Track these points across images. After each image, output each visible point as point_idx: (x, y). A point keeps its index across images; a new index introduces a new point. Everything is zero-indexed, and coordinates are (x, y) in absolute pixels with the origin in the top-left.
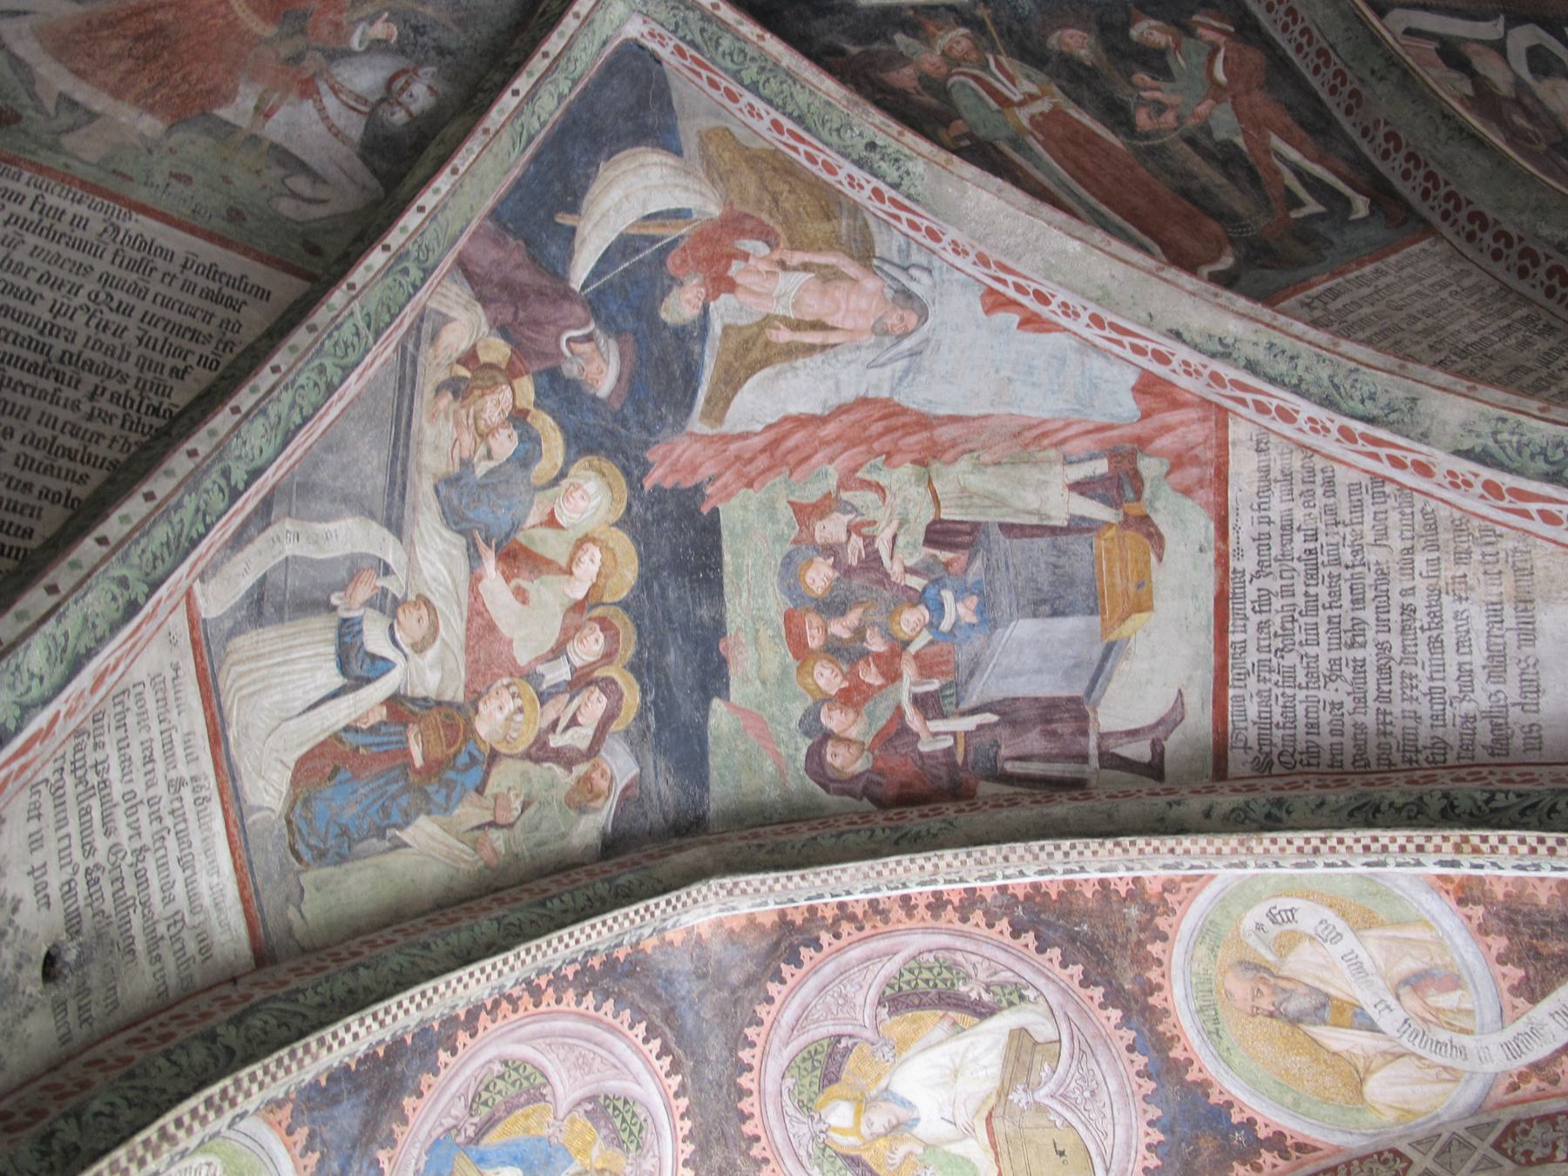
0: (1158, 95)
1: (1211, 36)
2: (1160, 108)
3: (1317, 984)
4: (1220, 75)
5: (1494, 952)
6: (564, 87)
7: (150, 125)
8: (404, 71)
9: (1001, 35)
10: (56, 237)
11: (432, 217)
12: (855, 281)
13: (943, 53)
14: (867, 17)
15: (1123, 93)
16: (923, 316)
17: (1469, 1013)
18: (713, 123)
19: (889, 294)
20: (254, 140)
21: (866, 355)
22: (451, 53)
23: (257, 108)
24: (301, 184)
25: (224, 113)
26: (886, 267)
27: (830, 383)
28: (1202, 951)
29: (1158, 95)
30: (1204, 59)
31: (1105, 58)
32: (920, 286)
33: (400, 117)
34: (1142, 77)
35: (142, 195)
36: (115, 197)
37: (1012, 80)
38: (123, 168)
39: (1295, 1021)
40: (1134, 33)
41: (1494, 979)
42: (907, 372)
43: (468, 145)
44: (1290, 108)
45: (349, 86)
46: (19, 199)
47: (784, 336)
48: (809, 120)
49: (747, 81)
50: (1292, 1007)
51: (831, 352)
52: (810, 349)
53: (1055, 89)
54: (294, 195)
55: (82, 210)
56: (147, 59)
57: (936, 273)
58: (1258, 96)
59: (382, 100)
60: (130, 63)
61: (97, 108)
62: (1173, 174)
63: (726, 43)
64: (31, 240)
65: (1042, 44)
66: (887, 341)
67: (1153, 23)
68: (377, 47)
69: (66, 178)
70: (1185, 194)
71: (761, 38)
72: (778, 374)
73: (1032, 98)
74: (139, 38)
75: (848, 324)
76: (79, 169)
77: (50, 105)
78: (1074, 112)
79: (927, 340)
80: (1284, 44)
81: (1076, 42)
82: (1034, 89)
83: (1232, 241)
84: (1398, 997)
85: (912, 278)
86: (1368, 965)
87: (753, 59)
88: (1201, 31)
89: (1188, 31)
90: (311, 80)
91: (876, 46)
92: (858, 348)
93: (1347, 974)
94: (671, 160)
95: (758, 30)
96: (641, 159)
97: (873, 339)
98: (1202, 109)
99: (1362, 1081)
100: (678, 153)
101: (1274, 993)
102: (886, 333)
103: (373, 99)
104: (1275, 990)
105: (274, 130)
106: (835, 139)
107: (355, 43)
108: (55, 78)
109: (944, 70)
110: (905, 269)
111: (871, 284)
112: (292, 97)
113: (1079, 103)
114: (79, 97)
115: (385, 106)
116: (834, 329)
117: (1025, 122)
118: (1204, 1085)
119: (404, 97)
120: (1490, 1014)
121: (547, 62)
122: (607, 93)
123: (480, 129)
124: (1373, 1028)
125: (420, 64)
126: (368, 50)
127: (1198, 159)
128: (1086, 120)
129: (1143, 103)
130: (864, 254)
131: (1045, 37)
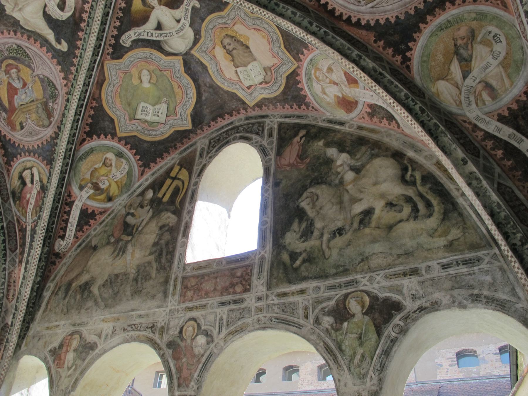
3: (474, 57)
5: (511, 106)
17: (485, 104)
28: (473, 15)
39: (457, 53)
41: (501, 108)
50: (462, 51)
84: (480, 82)
86: (488, 71)
93: (482, 65)
99: (443, 79)
101: (465, 44)
104: (466, 45)
118: (420, 31)
120: (486, 110)
124: (465, 77)
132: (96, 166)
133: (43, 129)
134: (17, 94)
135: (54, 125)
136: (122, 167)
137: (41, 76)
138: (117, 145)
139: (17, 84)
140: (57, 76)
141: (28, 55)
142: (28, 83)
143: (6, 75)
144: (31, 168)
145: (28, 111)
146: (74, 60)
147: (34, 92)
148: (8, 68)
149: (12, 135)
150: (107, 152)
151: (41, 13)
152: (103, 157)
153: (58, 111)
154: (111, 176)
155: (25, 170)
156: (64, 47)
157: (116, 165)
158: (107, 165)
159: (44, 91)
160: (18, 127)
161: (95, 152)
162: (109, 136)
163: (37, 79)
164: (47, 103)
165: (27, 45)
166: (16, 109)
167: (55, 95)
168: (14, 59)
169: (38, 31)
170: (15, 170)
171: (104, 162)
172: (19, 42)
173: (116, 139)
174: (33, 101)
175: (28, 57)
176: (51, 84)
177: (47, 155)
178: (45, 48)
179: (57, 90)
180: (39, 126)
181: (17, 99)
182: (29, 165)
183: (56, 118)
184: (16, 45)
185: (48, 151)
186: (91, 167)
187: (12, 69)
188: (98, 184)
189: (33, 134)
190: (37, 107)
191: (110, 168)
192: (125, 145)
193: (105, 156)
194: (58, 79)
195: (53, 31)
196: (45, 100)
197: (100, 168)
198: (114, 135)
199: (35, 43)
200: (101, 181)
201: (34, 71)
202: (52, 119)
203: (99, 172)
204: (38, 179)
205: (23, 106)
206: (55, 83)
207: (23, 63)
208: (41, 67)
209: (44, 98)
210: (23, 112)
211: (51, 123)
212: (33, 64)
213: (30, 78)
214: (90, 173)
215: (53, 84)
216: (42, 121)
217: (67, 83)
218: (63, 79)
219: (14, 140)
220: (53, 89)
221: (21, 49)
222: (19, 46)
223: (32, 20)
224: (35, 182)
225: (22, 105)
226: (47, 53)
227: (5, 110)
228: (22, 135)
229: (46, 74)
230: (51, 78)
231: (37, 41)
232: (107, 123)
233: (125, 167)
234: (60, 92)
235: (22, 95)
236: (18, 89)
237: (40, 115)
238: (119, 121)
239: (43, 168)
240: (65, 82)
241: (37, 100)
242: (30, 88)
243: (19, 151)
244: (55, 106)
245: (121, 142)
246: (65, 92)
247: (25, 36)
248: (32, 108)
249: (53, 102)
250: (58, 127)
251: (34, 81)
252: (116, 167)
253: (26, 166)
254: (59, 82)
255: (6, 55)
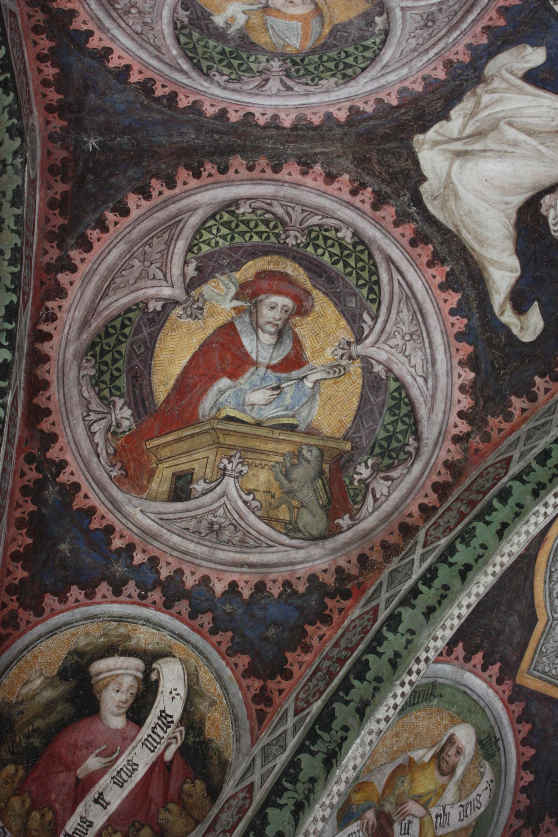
132: (416, 755)
133: (287, 540)
134: (234, 375)
135: (347, 544)
136: (474, 795)
137: (378, 368)
138: (499, 706)
139: (259, 346)
140: (440, 396)
141: (377, 282)
142: (312, 363)
143: (236, 297)
144: (150, 658)
145: (247, 450)
146: (537, 379)
147: (318, 402)
148: (264, 284)
149: (113, 501)
150: (464, 721)
151: (519, 200)
152: (446, 728)
153: (387, 507)
154: (434, 811)
155: (110, 650)
156: (529, 326)
157: (464, 776)
158: (444, 766)
159: (359, 415)
160: (161, 482)
161: (435, 702)
162: (494, 670)
163: (356, 368)
164: (349, 460)
165: (396, 254)
166: (192, 419)
167: (399, 450)
168: (314, 269)
169: (467, 237)
170: (52, 632)
171: (442, 750)
172: (370, 231)
173: (507, 686)
174: (292, 428)
175: (371, 291)
176: (404, 410)
177: (266, 639)
178: (457, 297)
179: (418, 439)
180: (268, 520)
181: (221, 392)
182: (144, 637)
183: (365, 525)
184: (355, 234)
185: (275, 624)
186: (403, 750)
187: (279, 293)
188: (391, 823)
189: (226, 535)
190: (298, 455)
191: (445, 779)
192: (519, 720)
193: (451, 731)
194: (440, 406)
195: (523, 266)
196: (348, 446)
197: (424, 766)
198: (509, 671)
199: (430, 264)
200: (404, 815)
201: (359, 340)
202: (345, 521)
203: (412, 780)
204: (175, 709)
205: (232, 426)
206: (423, 412)
207: (338, 299)
208: (398, 341)
209: (345, 438)
210: (220, 445)
211: (332, 531)
212: (375, 318)
213: (329, 354)
214: (389, 769)
215: (413, 412)
216: (291, 509)
217: (468, 435)
218: (461, 414)
219: (111, 519)
220: (401, 427)
221: (365, 257)
222: (362, 243)
223: (469, 199)
224: (152, 719)
225: (229, 419)
226: (452, 312)
227: (141, 401)
228: (164, 521)
229: (401, 369)
230: (415, 392)
231: (443, 262)
232: (514, 620)
233: (482, 793)
234: (426, 452)
235: (255, 388)
236: (255, 364)
237: (295, 486)
238: (547, 634)
239: (219, 678)
240: (464, 427)
241: (311, 432)
242: (308, 384)
243: (119, 569)
244: (381, 487)
245: (513, 707)
246: (444, 456)
247: (408, 229)
248: (270, 446)
249: (376, 469)
250: (363, 559)
251: (337, 370)
252: (462, 783)
253: (129, 638)
254: (438, 416)
255: (291, 241)
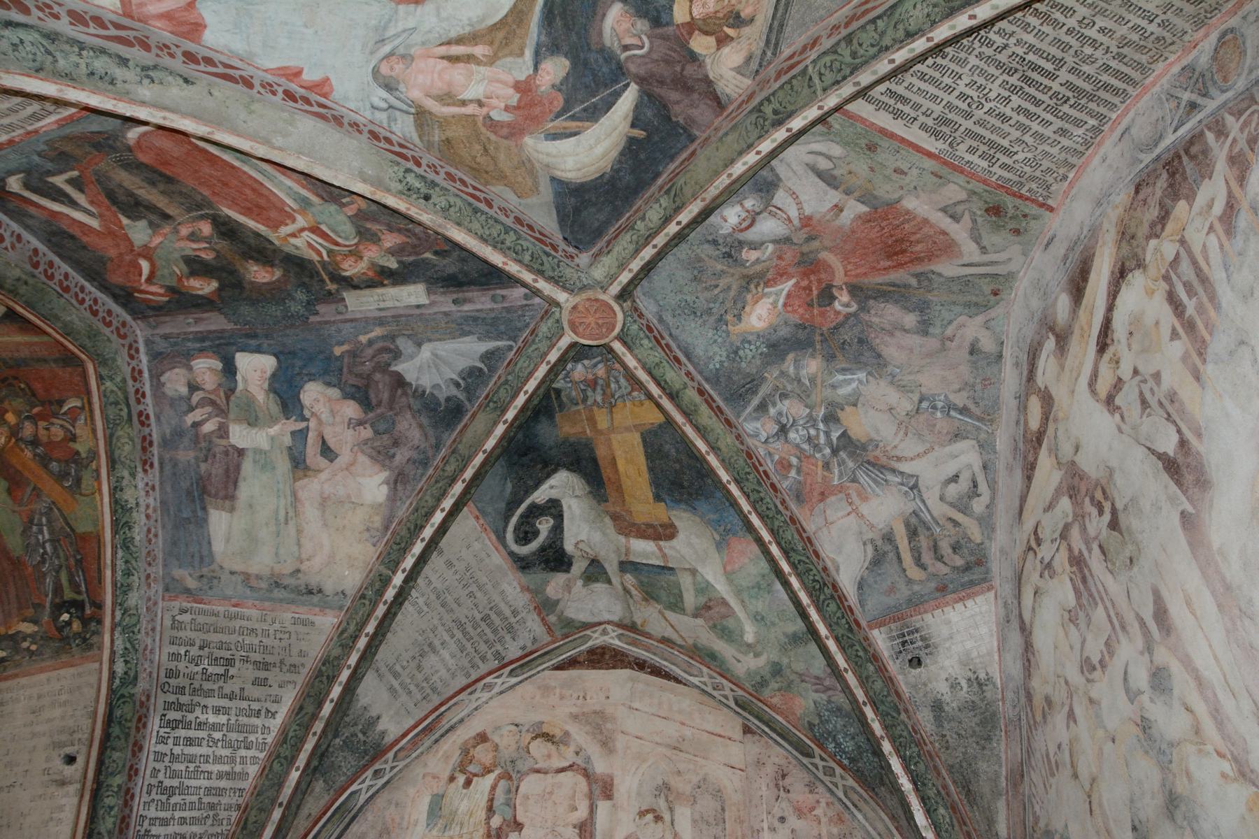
0: (195, 246)
1: (153, 289)
2: (193, 237)
4: (145, 265)
6: (640, 225)
7: (910, 203)
8: (742, 231)
9: (318, 273)
10: (991, 144)
11: (750, 147)
12: (428, 96)
13: (361, 258)
14: (418, 277)
15: (223, 245)
16: (376, 72)
18: (529, 201)
19: (402, 87)
20: (848, 192)
21: (417, 38)
22: (708, 241)
23: (842, 211)
24: (823, 164)
25: (863, 209)
26: (405, 107)
27: (444, 14)
29: (195, 246)
30: (158, 273)
31: (238, 267)
32: (379, 96)
33: (749, 204)
34: (208, 256)
35: (929, 164)
36: (946, 163)
37: (310, 245)
38: (935, 180)
40: (215, 284)
42: (385, 28)
43: (717, 192)
44: (84, 247)
45: (779, 222)
46: (1004, 166)
47: (480, 50)
48: (469, 210)
49: (512, 233)
51: (444, 39)
52: (459, 41)
53: (276, 242)
54: (829, 158)
55: (968, 157)
56: (902, 240)
57: (368, 106)
58: (113, 253)
59: (759, 214)
60: (913, 238)
61: (940, 214)
62: (181, 193)
63: (527, 258)
64: (1005, 143)
65: (286, 271)
66: (401, 50)
67: (200, 293)
68: (754, 246)
69: (972, 176)
70: (170, 180)
71: (505, 263)
72: (483, 20)
73: (293, 235)
74: (903, 252)
75: (432, 61)
76: (961, 179)
77: (967, 217)
78: (261, 229)
79: (372, 53)
80: (93, 290)
81: (259, 274)
82: (293, 240)
83: (130, 149)
85: (385, 100)
87: (509, 249)
88: (162, 291)
89: (171, 290)
90: (804, 226)
91: (411, 259)
92: (423, 43)
94: (558, 174)
95: (507, 268)
96: (580, 174)
97: (412, 51)
98: (157, 240)
100: (553, 179)
102: (403, 57)
103: (765, 214)
105: (834, 197)
106: (452, 200)
107: (771, 247)
108: (959, 232)
109: (361, 247)
110: (391, 107)
111: (416, 94)
112: (818, 216)
113: (257, 235)
114: (949, 220)
115: (758, 210)
116: (443, 58)
117: (299, 218)
119: (744, 215)
121: (654, 242)
122: (602, 217)
123: (707, 201)
125: (730, 235)
126: (763, 244)
127: (160, 205)
128: (252, 224)
129: (207, 240)
130: (421, 116)
131: (284, 275)
